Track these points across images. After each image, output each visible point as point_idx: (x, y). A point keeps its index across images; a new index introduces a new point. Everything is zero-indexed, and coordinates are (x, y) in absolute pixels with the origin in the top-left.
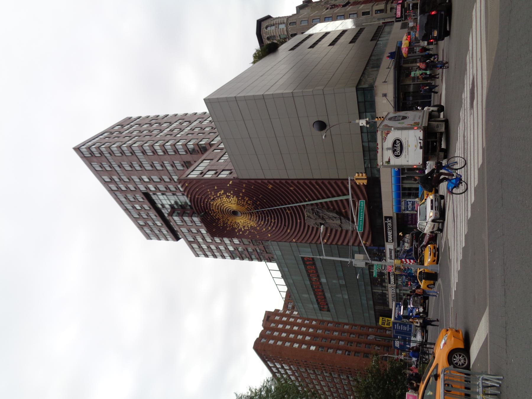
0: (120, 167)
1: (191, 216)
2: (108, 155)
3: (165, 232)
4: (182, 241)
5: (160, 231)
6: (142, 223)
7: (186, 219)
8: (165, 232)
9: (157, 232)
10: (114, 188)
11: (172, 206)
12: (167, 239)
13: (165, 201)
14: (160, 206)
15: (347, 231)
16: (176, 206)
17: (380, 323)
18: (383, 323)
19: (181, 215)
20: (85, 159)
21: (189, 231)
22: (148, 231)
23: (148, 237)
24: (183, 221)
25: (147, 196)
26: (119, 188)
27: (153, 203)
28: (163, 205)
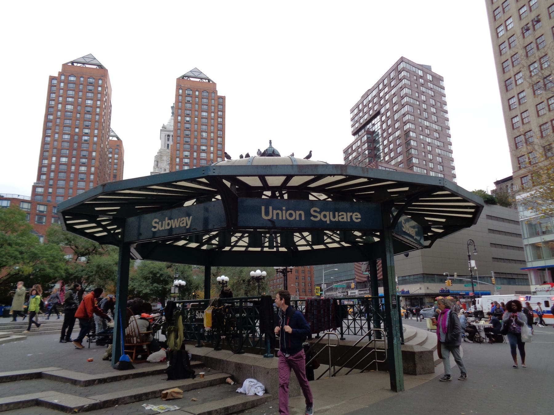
0: (394, 94)
1: (368, 148)
2: (400, 85)
3: (357, 125)
4: (353, 138)
5: (357, 122)
6: (361, 107)
7: (366, 145)
8: (357, 125)
9: (356, 119)
10: (381, 86)
11: (374, 132)
12: (353, 126)
13: (377, 125)
14: (373, 122)
15: (361, 267)
16: (374, 135)
17: (317, 287)
18: (317, 289)
19: (368, 141)
20: (396, 65)
21: (359, 147)
22: (356, 111)
23: (352, 111)
24: (364, 143)
25: (378, 113)
26: (380, 91)
27: (374, 117)
28: (374, 125)
